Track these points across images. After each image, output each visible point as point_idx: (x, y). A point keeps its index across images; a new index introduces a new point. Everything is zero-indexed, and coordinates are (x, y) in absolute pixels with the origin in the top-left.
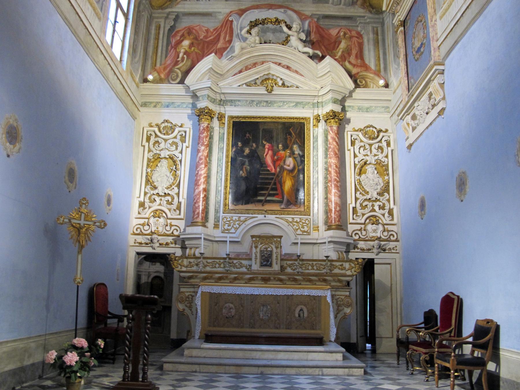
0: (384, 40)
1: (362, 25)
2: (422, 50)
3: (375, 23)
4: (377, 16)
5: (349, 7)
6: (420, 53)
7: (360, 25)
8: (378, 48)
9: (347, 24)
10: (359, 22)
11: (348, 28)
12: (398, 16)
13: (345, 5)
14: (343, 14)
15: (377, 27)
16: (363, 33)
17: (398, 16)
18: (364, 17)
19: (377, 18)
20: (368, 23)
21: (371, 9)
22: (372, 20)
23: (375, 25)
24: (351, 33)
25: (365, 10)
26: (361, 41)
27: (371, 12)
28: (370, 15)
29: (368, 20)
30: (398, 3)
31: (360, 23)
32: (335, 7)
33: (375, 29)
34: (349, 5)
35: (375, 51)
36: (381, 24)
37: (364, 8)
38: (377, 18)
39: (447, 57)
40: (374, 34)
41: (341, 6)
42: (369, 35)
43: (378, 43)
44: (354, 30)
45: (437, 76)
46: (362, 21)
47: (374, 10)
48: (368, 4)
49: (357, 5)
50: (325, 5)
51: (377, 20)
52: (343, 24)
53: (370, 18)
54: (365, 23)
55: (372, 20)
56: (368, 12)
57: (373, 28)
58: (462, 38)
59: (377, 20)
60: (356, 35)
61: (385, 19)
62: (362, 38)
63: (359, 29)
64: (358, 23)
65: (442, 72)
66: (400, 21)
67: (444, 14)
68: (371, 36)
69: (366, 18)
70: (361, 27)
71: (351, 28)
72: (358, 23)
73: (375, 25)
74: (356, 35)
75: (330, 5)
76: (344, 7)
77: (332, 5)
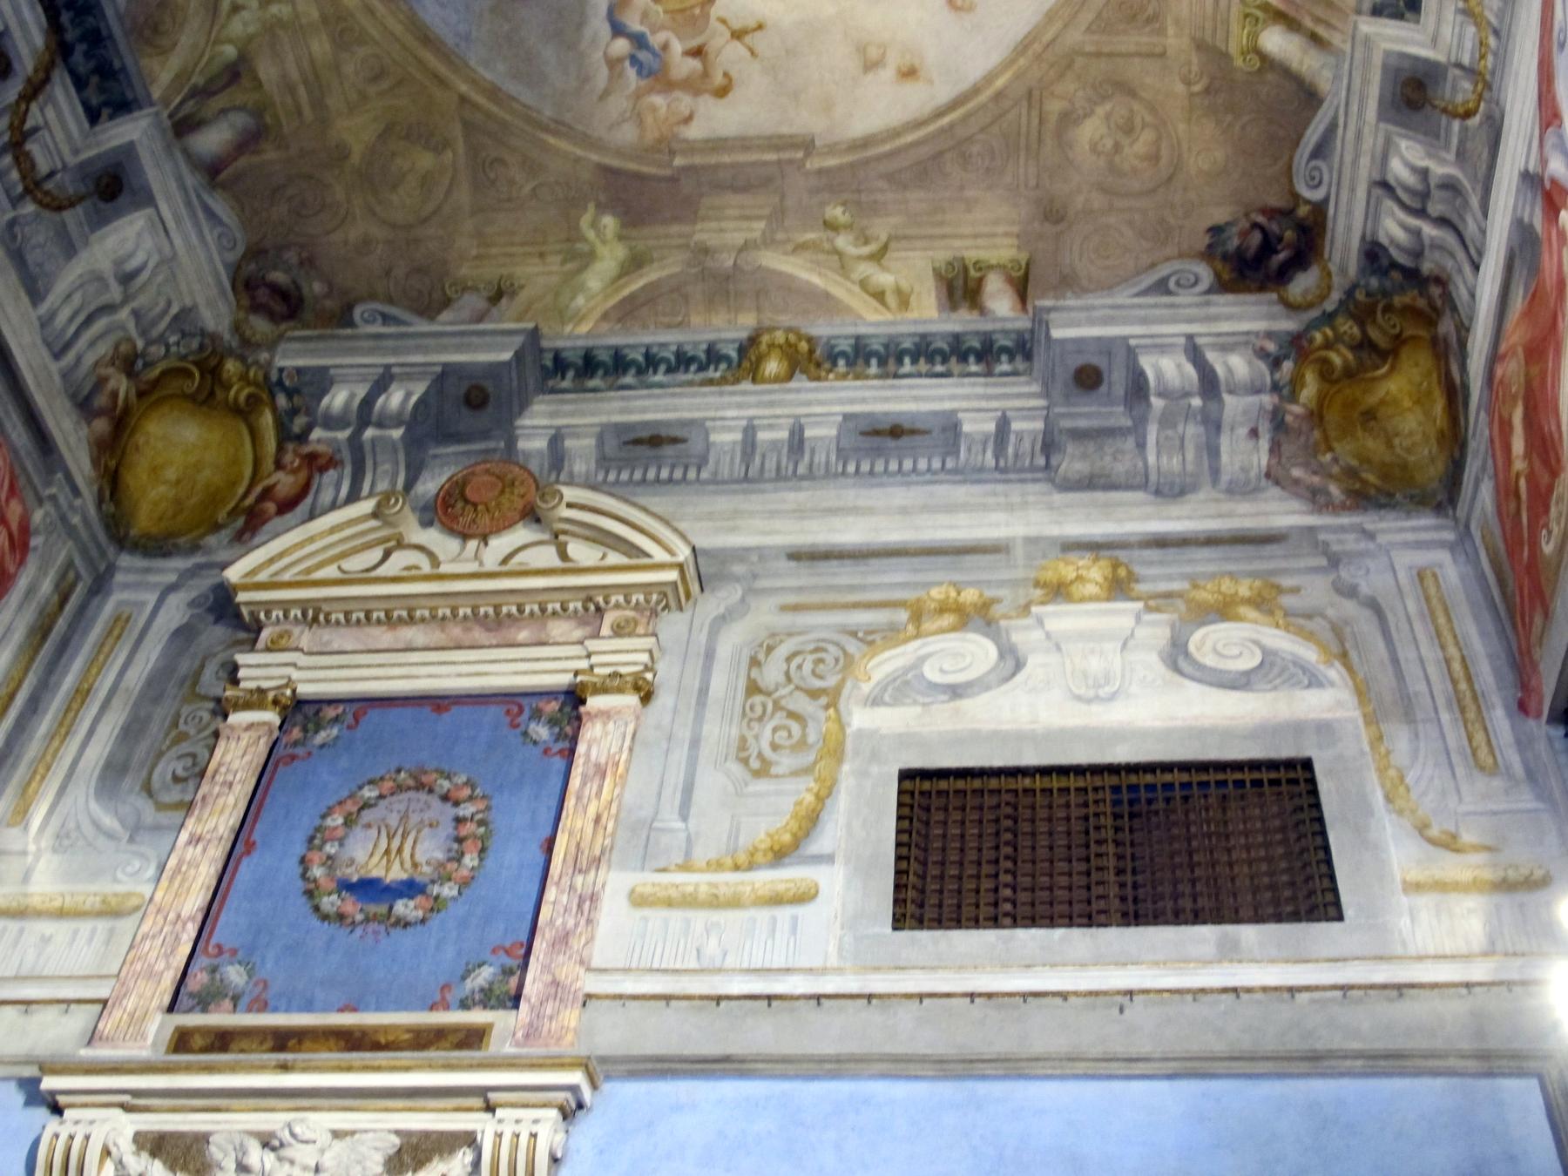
0: (63, 646)
1: (53, 511)
2: (403, 907)
3: (84, 551)
4: (102, 536)
5: (68, 404)
6: (382, 909)
7: (48, 507)
8: (32, 659)
9: (23, 453)
10: (54, 490)
11: (18, 471)
12: (294, 665)
13: (65, 375)
14: (40, 400)
15: (78, 577)
16: (35, 549)
17: (294, 665)
18: (76, 491)
19: (99, 546)
20: (71, 531)
21: (107, 493)
22: (84, 534)
23: (78, 561)
24: (7, 500)
25: (93, 474)
26: (12, 569)
27: (100, 501)
28: (92, 511)
29: (76, 520)
30: (315, 619)
31: (53, 498)
32: (39, 342)
33: (71, 575)
34: (73, 397)
35: (16, 658)
36: (95, 581)
37: (95, 462)
38: (99, 546)
39: (633, 1075)
40: (57, 586)
41: (55, 367)
42: (45, 574)
43: (44, 637)
44: (23, 502)
45: (544, 1106)
46: (62, 500)
47: (112, 509)
48: (112, 464)
49: (89, 423)
50: (23, 294)
51: (94, 553)
52: (14, 436)
53: (85, 520)
54: (63, 519)
55: (84, 534)
56: (95, 488)
57: (69, 565)
58: (785, 1077)
59: (94, 553)
60: (14, 526)
61: (119, 578)
62: (21, 563)
63: (38, 517)
64: (48, 492)
65: (571, 1111)
66: (294, 691)
67: (669, 903)
68: (46, 586)
69: (78, 502)
70: (47, 514)
71: (22, 481)
72: (48, 492)
73: (78, 561)
74: (14, 526)
75: (33, 315)
76: (57, 379)
77: (37, 324)
